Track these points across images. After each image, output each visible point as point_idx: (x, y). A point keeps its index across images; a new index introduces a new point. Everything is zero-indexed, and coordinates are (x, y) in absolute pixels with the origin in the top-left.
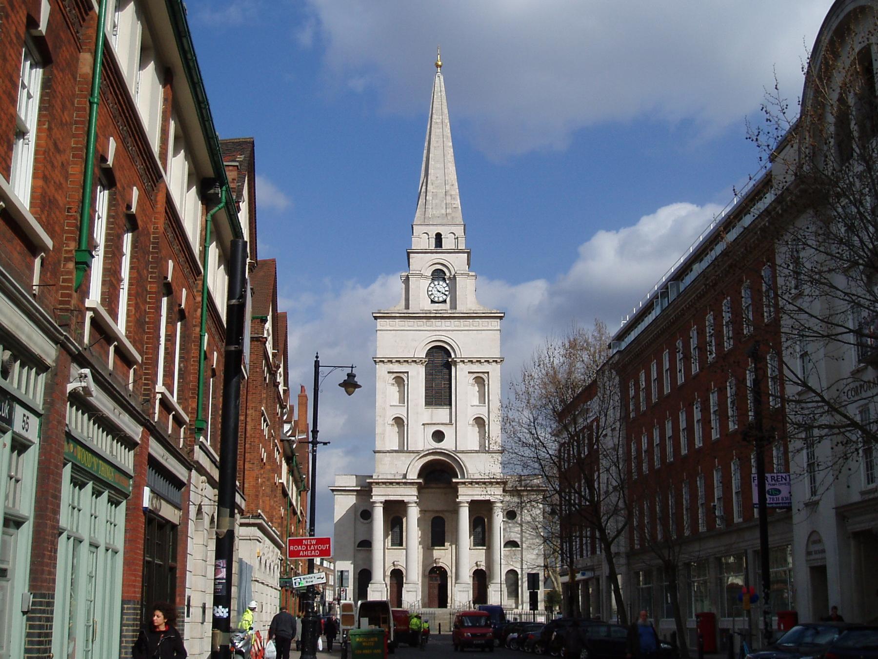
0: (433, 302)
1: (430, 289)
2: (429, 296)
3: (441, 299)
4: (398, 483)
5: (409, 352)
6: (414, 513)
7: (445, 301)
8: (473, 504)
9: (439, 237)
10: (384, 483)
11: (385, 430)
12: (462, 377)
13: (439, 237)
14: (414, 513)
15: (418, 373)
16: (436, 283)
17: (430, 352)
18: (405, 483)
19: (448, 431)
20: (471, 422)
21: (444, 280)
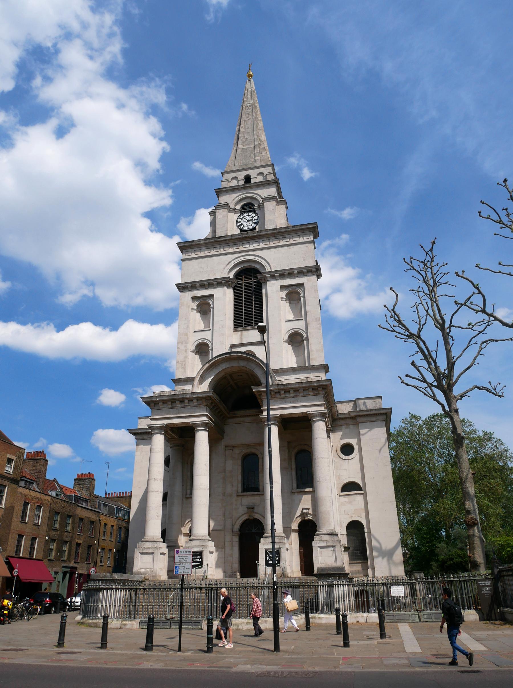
0: (241, 231)
1: (239, 220)
2: (239, 226)
3: (250, 227)
4: (182, 401)
5: (215, 274)
6: (202, 439)
7: (254, 229)
8: (286, 423)
9: (248, 179)
10: (164, 402)
11: (186, 357)
12: (273, 293)
13: (248, 179)
14: (202, 439)
15: (225, 294)
16: (245, 214)
17: (238, 275)
18: (190, 400)
20: (286, 338)
21: (254, 211)
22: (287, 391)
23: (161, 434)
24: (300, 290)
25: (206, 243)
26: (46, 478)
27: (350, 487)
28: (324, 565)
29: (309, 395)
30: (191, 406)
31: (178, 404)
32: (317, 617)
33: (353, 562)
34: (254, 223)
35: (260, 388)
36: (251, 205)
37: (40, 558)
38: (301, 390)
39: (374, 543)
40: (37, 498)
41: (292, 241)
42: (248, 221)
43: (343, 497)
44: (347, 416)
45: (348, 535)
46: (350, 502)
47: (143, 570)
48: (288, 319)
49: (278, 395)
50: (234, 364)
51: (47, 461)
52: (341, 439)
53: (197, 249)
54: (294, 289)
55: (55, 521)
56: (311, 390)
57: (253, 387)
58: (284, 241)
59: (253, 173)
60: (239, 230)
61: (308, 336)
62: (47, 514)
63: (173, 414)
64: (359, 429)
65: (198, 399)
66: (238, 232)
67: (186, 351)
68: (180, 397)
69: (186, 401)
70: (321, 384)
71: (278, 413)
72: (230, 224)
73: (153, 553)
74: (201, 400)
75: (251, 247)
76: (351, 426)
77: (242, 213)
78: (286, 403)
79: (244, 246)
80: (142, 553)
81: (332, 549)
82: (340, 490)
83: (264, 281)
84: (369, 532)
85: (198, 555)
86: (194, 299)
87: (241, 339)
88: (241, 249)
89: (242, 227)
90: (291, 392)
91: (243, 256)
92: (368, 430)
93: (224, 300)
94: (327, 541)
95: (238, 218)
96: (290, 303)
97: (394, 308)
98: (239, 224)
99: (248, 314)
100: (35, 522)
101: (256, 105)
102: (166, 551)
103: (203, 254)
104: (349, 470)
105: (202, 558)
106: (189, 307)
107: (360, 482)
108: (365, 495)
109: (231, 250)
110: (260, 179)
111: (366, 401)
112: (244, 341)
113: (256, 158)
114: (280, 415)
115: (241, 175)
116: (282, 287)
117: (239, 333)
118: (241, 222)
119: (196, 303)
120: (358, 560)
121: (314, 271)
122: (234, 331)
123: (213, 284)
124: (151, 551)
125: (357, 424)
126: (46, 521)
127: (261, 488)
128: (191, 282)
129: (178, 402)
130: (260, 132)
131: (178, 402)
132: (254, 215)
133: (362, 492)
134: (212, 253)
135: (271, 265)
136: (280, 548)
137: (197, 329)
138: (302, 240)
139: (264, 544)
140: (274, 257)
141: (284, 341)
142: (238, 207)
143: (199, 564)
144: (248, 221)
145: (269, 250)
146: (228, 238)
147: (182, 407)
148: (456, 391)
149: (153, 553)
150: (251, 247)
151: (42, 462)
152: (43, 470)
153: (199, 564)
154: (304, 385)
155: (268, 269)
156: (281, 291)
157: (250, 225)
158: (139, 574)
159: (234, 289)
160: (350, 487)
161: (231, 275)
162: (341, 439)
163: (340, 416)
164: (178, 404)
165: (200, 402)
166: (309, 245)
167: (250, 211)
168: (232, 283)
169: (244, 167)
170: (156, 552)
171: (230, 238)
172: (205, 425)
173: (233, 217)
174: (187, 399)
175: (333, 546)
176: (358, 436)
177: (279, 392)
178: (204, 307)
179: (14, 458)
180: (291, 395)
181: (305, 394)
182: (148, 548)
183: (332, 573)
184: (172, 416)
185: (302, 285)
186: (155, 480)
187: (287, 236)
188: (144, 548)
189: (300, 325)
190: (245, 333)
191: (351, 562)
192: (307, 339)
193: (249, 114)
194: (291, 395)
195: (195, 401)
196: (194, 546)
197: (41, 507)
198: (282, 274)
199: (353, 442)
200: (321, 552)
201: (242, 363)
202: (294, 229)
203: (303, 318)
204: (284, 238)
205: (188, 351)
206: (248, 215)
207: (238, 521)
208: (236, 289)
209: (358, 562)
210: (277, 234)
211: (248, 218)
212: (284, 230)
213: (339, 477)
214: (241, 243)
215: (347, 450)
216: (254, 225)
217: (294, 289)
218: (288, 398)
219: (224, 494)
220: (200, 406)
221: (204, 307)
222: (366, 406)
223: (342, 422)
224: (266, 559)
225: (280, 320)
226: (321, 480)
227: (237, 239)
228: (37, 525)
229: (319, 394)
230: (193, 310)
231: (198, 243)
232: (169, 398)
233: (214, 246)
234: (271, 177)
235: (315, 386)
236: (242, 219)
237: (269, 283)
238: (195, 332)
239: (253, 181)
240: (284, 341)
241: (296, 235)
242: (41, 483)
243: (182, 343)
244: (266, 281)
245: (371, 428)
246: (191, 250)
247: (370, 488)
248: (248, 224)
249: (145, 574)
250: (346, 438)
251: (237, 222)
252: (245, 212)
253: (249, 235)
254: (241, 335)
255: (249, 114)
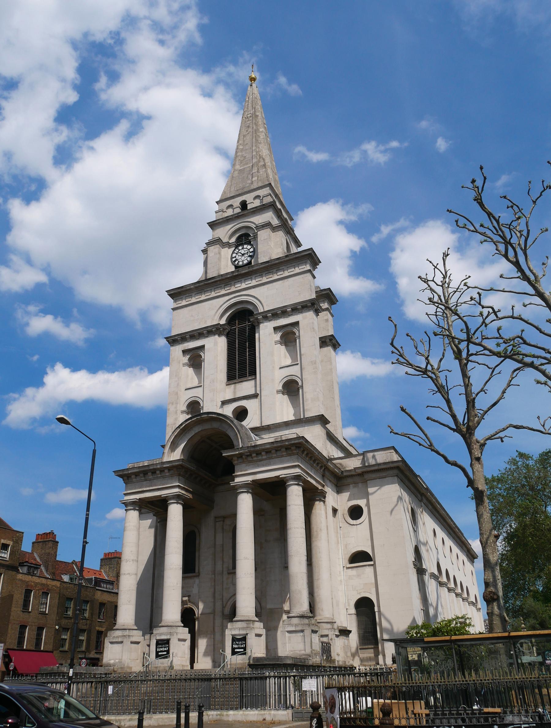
0: (237, 267)
1: (234, 255)
2: (233, 263)
3: (246, 262)
4: (154, 472)
5: (206, 322)
6: (175, 513)
7: (250, 263)
9: (244, 205)
12: (267, 336)
13: (244, 205)
14: (175, 513)
15: (216, 344)
16: (240, 248)
18: (162, 470)
19: (251, 405)
20: (280, 388)
21: (249, 243)
22: (258, 453)
23: (134, 509)
24: (295, 330)
25: (196, 288)
26: (58, 559)
27: (360, 557)
28: (292, 653)
29: (282, 456)
30: (164, 477)
31: (150, 475)
32: (225, 713)
33: (364, 647)
34: (250, 256)
35: (229, 452)
36: (247, 235)
37: (50, 650)
38: (273, 451)
39: (385, 624)
40: (42, 584)
41: (286, 274)
42: (243, 255)
43: (350, 570)
44: (353, 473)
45: (358, 614)
46: (358, 576)
47: (112, 662)
48: (283, 364)
49: (250, 459)
50: (207, 426)
51: (58, 542)
52: (348, 500)
53: (187, 295)
54: (289, 329)
55: (67, 608)
56: (284, 449)
57: (222, 451)
58: (279, 274)
59: (248, 198)
60: (234, 267)
61: (302, 384)
62: (57, 601)
63: (146, 487)
64: (367, 487)
65: (169, 469)
66: (233, 269)
67: (176, 413)
68: (151, 468)
69: (158, 472)
70: (293, 442)
71: (250, 478)
72: (224, 262)
73: (122, 642)
74: (174, 469)
75: (244, 286)
76: (360, 485)
77: (237, 247)
78: (259, 466)
79: (236, 286)
80: (112, 643)
81: (302, 634)
82: (347, 561)
83: (256, 324)
84: (379, 611)
85: (165, 644)
86: (185, 352)
87: (235, 392)
88: (233, 289)
89: (236, 263)
90: (263, 453)
91: (235, 297)
92: (377, 488)
93: (216, 349)
94: (296, 625)
95: (233, 253)
96: (286, 345)
97: (392, 342)
98: (234, 259)
99: (242, 363)
100: (42, 610)
101: (257, 114)
102: (263, 632)
103: (194, 300)
104: (357, 537)
105: (169, 647)
106: (179, 363)
107: (370, 551)
108: (374, 565)
109: (223, 292)
110: (257, 203)
111: (376, 453)
112: (239, 395)
113: (254, 179)
114: (253, 481)
115: (237, 202)
116: (276, 329)
117: (233, 386)
118: (235, 257)
119: (280, 334)
120: (370, 644)
121: (310, 307)
122: (227, 385)
123: (203, 333)
124: (120, 640)
125: (365, 482)
126: (55, 609)
127: (197, 570)
128: (181, 334)
129: (150, 474)
130: (260, 146)
131: (150, 474)
132: (249, 247)
133: (372, 563)
134: (203, 297)
135: (263, 302)
136: (247, 634)
137: (283, 365)
138: (297, 270)
139: (231, 629)
140: (267, 295)
141: (278, 392)
142: (233, 240)
143: (165, 653)
144: (243, 255)
145: (263, 287)
146: (218, 279)
147: (154, 479)
148: (480, 434)
149: (122, 642)
150: (244, 286)
151: (50, 544)
152: (53, 552)
153: (165, 653)
154: (275, 445)
155: (261, 310)
156: (275, 333)
157: (245, 260)
158: (109, 665)
159: (227, 336)
160: (360, 557)
161: (223, 321)
162: (348, 500)
163: (345, 474)
164: (150, 475)
165: (172, 472)
166: (305, 275)
167: (245, 244)
168: (224, 329)
169: (240, 192)
170: (125, 640)
171: (221, 278)
172: (178, 498)
173: (227, 252)
174: (158, 469)
175: (302, 631)
176: (366, 496)
177: (251, 455)
178: (195, 360)
179: (11, 543)
180: (264, 457)
181: (278, 454)
182: (118, 637)
183: (267, 663)
184: (145, 489)
185: (297, 324)
186: (127, 561)
187: (281, 268)
188: (114, 637)
189: (295, 371)
190: (239, 386)
191: (362, 647)
192: (302, 387)
193: (249, 127)
194: (264, 457)
195: (166, 471)
196: (161, 634)
197: (48, 594)
198: (276, 314)
199: (362, 503)
200: (289, 637)
201: (215, 425)
202: (287, 258)
203: (299, 362)
204: (278, 270)
205: (179, 412)
206: (243, 248)
207: (229, 603)
208: (230, 336)
209: (370, 647)
210: (273, 266)
211: (243, 252)
212: (277, 262)
213: (346, 546)
214: (233, 283)
215: (356, 513)
216: (249, 259)
217: (289, 329)
218: (261, 460)
219: (214, 572)
220: (172, 476)
221: (195, 360)
222: (376, 460)
223: (349, 480)
224: (232, 646)
225: (273, 367)
226: (292, 554)
227: (228, 278)
228: (44, 613)
229: (293, 454)
230: (184, 365)
231: (188, 288)
232: (141, 470)
233: (205, 290)
234: (268, 200)
235: (287, 445)
236: (237, 254)
237: (261, 325)
238: (186, 389)
239: (249, 207)
240: (278, 392)
241: (291, 265)
242: (50, 567)
243: (172, 404)
244: (259, 323)
245: (381, 486)
246: (181, 297)
247: (379, 558)
248: (243, 258)
249: (114, 665)
250: (354, 499)
251: (232, 258)
252: (239, 245)
253: (239, 273)
254: (235, 388)
255: (249, 127)
